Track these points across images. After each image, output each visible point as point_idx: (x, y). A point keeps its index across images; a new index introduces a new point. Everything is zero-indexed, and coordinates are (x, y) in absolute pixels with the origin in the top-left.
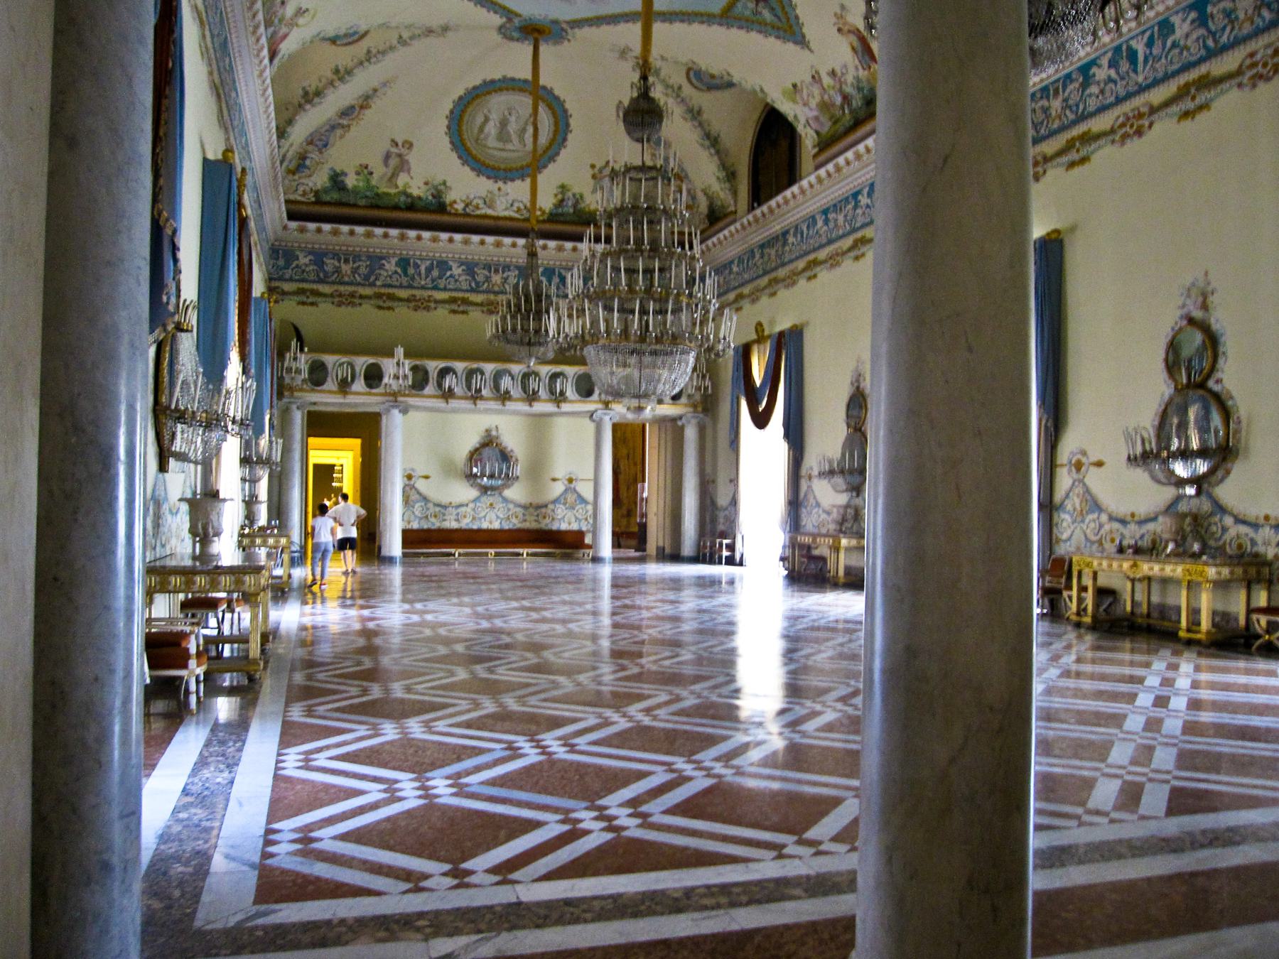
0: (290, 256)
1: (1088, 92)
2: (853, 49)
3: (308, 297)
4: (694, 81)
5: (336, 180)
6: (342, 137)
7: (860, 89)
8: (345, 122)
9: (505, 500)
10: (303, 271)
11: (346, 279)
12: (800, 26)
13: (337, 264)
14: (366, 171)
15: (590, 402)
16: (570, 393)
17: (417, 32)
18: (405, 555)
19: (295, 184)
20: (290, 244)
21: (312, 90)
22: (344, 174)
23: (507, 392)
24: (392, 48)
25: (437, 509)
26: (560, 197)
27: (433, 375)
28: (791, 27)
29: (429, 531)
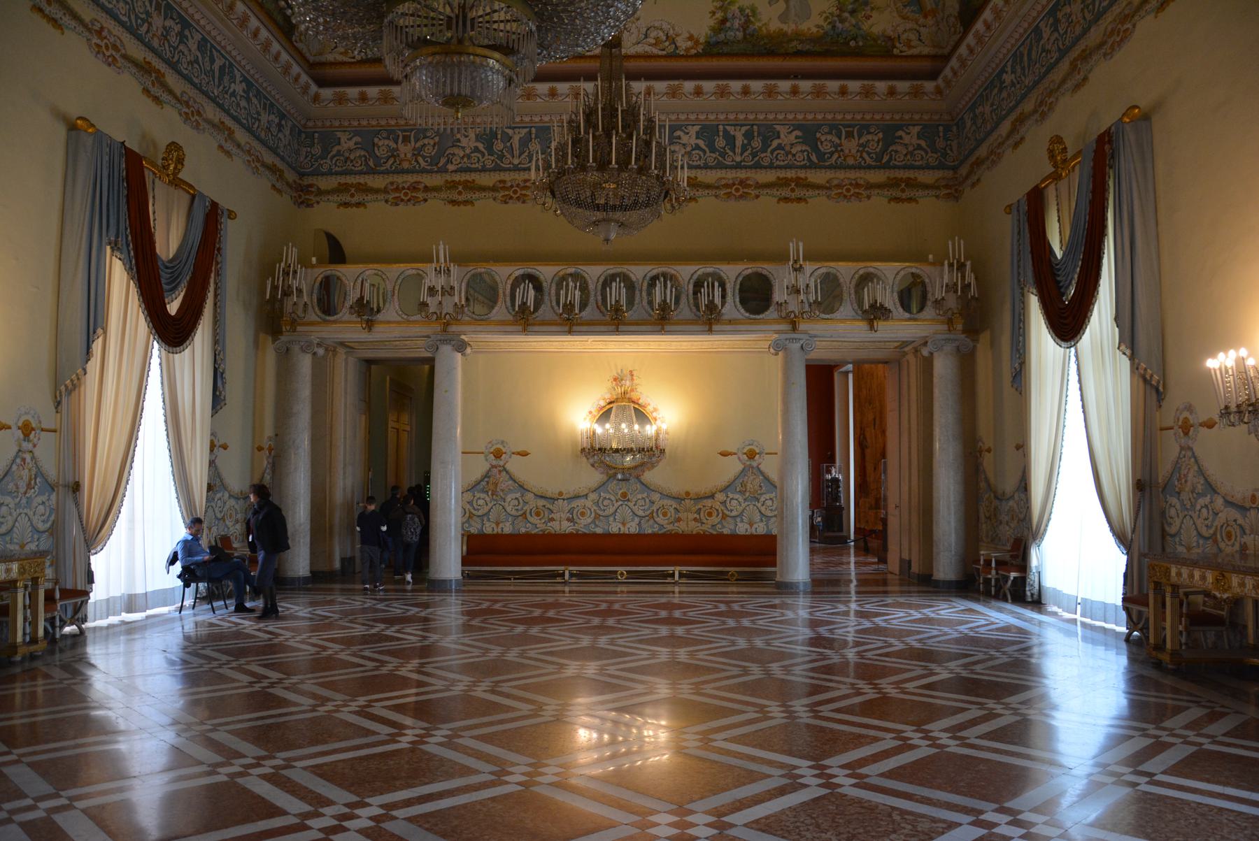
0: (329, 140)
3: (352, 196)
10: (347, 158)
11: (406, 165)
13: (393, 145)
15: (766, 322)
16: (732, 308)
20: (328, 124)
23: (617, 309)
25: (541, 502)
26: (719, 15)
27: (504, 288)
29: (528, 536)
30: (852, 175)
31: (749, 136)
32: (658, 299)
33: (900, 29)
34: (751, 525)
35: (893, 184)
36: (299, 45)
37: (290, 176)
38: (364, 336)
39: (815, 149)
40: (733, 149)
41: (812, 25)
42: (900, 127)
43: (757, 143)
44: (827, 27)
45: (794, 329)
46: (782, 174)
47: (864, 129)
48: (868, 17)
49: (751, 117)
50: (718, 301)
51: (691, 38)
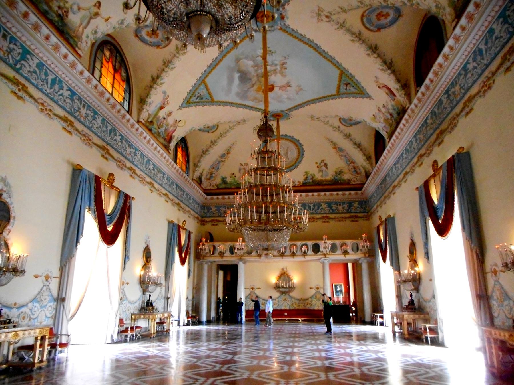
0: (209, 208)
1: (467, 77)
2: (387, 93)
4: (343, 123)
5: (224, 180)
6: (223, 165)
7: (394, 110)
8: (223, 159)
9: (291, 297)
10: (214, 213)
12: (365, 90)
14: (233, 176)
16: (310, 252)
17: (235, 124)
18: (246, 321)
19: (210, 183)
21: (205, 150)
22: (226, 178)
23: (282, 253)
24: (228, 131)
26: (306, 176)
28: (362, 91)
30: (341, 215)
31: (314, 206)
32: (292, 251)
33: (352, 178)
34: (318, 307)
35: (351, 217)
36: (202, 186)
37: (200, 218)
38: (221, 260)
39: (331, 208)
40: (310, 209)
41: (329, 177)
42: (353, 202)
43: (316, 208)
44: (333, 178)
45: (326, 257)
46: (323, 215)
47: (344, 203)
48: (343, 175)
49: (315, 201)
50: (306, 251)
51: (299, 182)
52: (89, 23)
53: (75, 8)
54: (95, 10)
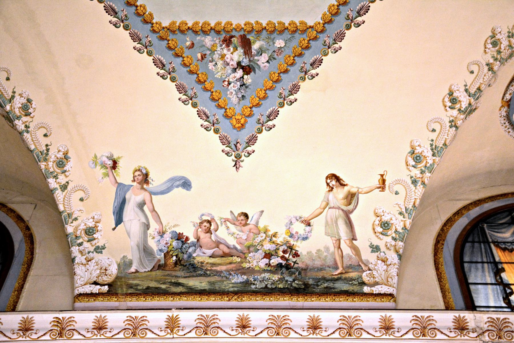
52: (350, 224)
53: (299, 228)
54: (340, 193)
